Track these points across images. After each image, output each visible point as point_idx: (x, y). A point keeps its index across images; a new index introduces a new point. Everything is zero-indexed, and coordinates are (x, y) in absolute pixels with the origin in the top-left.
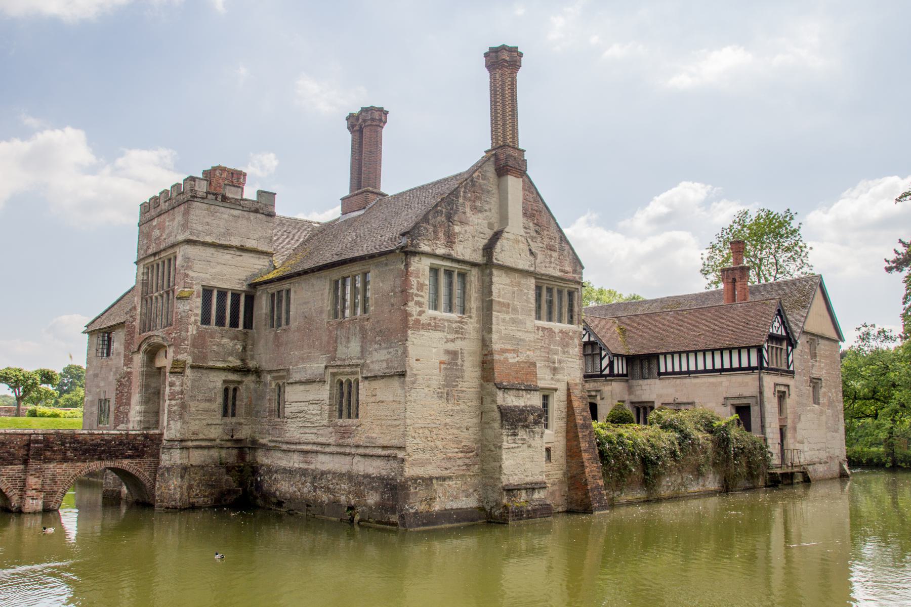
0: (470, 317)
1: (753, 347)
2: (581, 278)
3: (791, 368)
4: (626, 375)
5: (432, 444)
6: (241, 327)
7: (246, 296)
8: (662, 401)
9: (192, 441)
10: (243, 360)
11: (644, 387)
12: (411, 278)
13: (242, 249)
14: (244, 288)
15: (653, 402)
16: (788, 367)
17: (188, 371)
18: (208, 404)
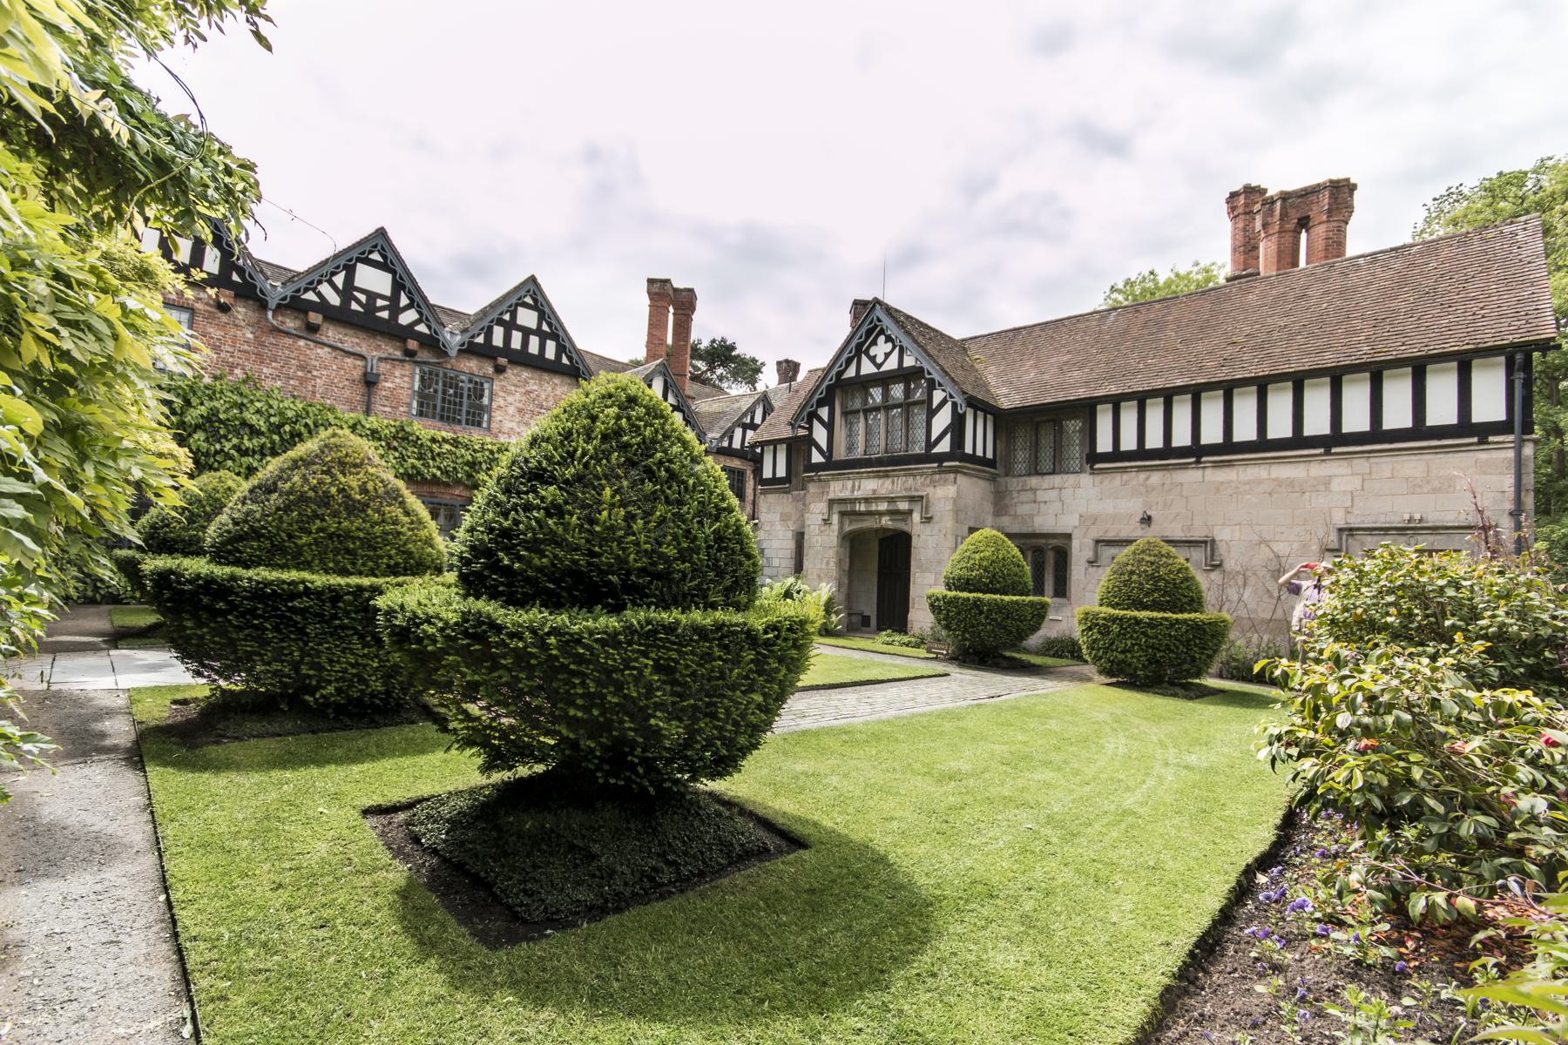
8: (1096, 533)
11: (1041, 496)
15: (1068, 536)
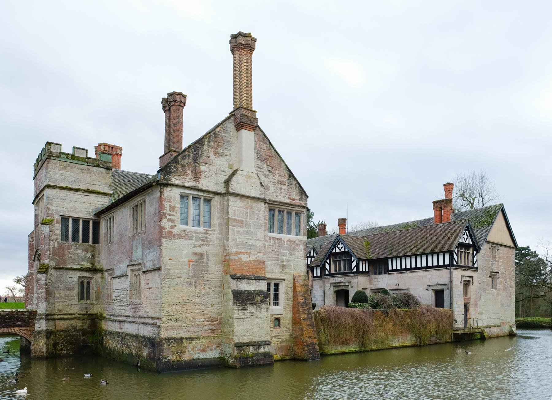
0: (214, 230)
1: (447, 252)
2: (306, 204)
3: (475, 266)
4: (368, 272)
5: (183, 316)
6: (91, 242)
7: (94, 223)
9: (58, 315)
10: (92, 264)
12: (164, 203)
13: (89, 191)
14: (92, 217)
16: (473, 264)
17: (52, 271)
18: (69, 292)
